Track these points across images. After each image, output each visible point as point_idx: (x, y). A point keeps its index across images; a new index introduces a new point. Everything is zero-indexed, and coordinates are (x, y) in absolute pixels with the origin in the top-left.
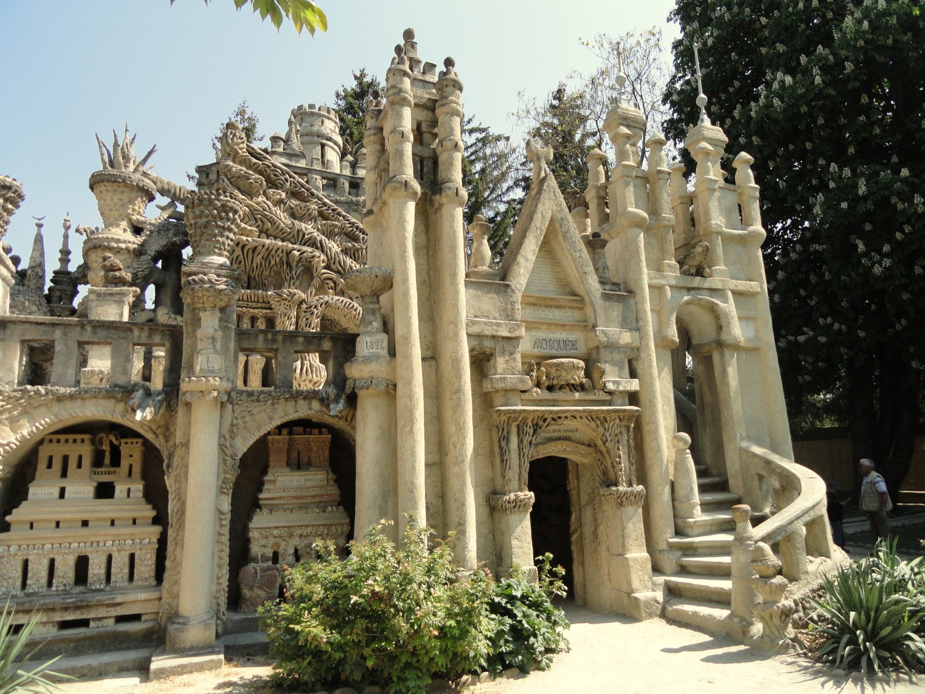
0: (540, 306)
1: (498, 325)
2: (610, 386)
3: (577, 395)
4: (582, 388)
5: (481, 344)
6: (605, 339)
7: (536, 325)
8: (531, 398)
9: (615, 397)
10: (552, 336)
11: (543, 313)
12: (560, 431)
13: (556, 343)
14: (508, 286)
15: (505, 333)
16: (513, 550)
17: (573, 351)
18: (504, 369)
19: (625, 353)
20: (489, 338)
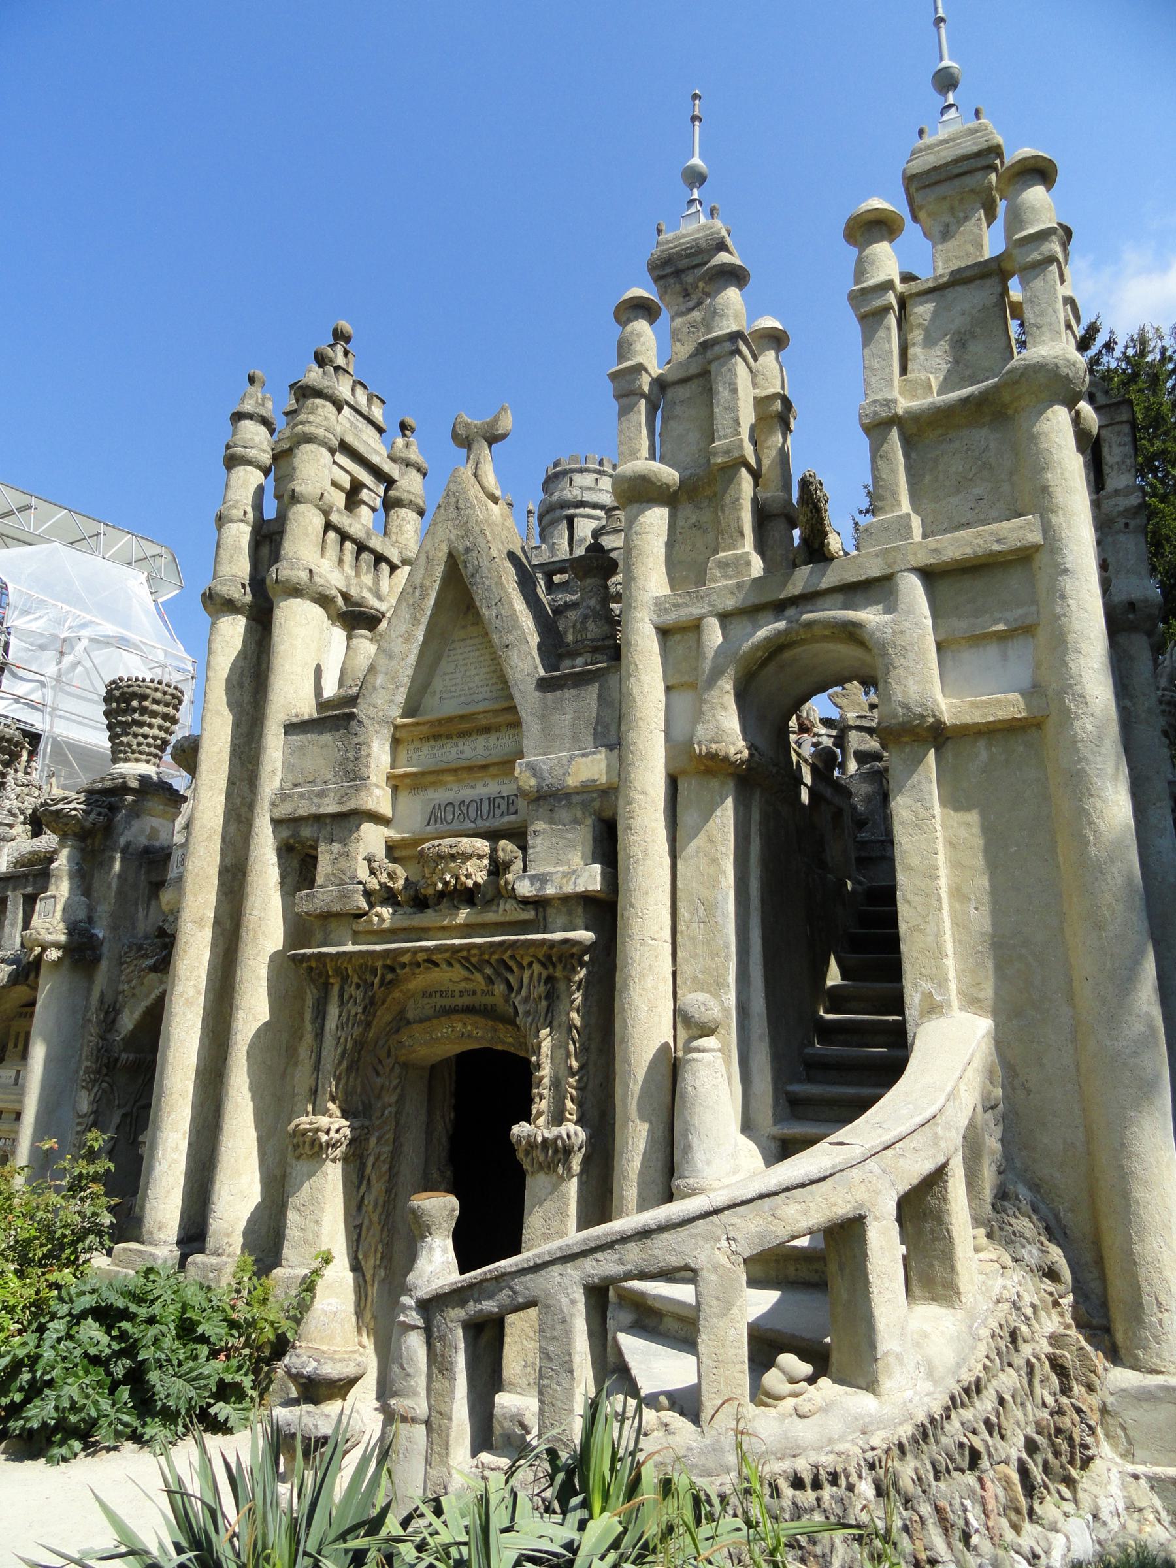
0: (449, 736)
1: (322, 794)
2: (525, 888)
3: (463, 915)
4: (468, 896)
5: (295, 835)
6: (533, 782)
7: (431, 778)
8: (369, 928)
9: (551, 912)
10: (467, 793)
11: (454, 750)
12: (474, 992)
13: (473, 808)
14: (352, 716)
15: (330, 807)
16: (287, 1231)
17: (506, 819)
18: (327, 875)
19: (585, 805)
20: (328, 821)
